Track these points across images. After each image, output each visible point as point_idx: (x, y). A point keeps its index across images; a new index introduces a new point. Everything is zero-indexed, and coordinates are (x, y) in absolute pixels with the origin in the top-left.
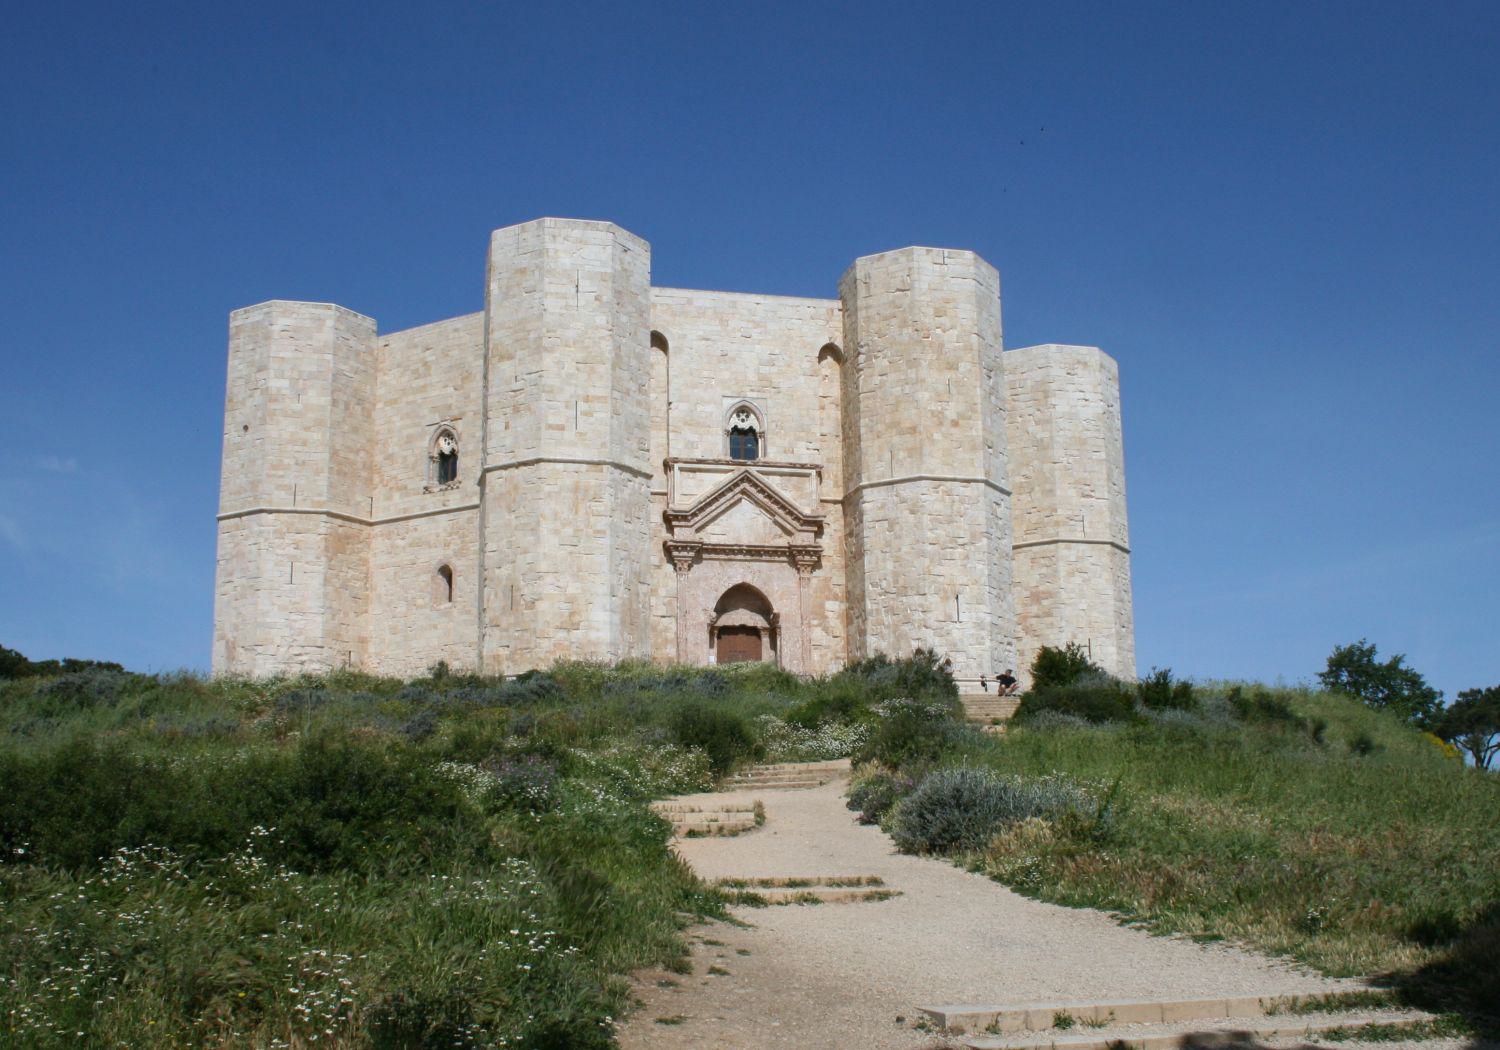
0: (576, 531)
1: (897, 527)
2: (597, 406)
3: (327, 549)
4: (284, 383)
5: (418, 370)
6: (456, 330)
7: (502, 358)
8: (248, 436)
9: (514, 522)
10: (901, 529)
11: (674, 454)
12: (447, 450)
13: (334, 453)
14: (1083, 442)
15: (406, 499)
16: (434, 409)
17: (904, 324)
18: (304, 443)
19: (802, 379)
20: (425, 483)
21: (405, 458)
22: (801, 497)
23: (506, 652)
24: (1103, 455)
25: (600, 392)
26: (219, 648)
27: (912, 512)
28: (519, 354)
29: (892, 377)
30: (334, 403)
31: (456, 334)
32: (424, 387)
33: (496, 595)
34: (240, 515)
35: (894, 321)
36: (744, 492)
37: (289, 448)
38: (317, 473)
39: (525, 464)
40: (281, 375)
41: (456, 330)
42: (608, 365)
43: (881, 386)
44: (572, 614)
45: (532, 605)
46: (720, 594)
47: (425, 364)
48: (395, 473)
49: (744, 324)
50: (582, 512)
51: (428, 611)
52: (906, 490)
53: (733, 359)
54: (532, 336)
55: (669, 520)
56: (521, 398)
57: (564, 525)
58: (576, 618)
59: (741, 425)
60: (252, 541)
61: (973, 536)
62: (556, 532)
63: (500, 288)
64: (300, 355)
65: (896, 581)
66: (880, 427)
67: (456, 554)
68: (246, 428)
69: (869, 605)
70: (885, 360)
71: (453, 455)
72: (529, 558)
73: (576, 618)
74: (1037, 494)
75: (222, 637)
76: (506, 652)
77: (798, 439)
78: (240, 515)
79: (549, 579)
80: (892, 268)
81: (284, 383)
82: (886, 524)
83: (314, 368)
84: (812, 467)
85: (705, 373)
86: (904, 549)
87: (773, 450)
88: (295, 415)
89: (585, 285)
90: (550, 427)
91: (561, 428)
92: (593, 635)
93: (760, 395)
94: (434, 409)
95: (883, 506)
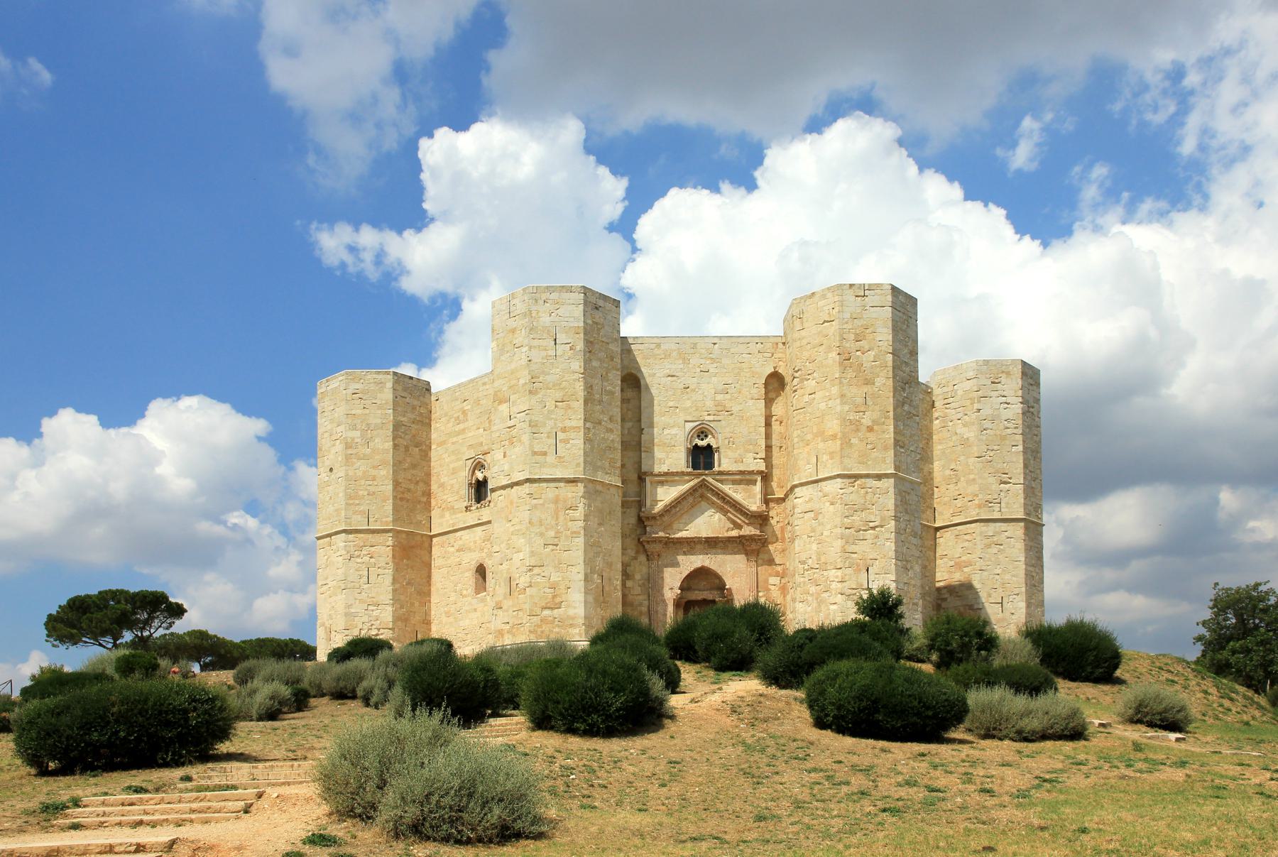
0: (558, 532)
1: (820, 517)
2: (573, 435)
3: (394, 556)
4: (358, 433)
6: (484, 384)
7: (501, 402)
11: (644, 468)
12: (480, 476)
13: (396, 484)
14: (1003, 438)
18: (374, 480)
19: (751, 402)
20: (466, 504)
21: (452, 486)
22: (749, 497)
23: (508, 627)
24: (1020, 448)
25: (574, 423)
26: (320, 632)
27: (832, 504)
30: (395, 446)
34: (330, 535)
36: (702, 496)
37: (363, 482)
38: (384, 501)
41: (484, 384)
42: (582, 401)
43: (810, 403)
44: (554, 597)
46: (684, 575)
47: (464, 412)
49: (703, 361)
50: (561, 518)
53: (693, 390)
54: (522, 381)
55: (643, 522)
56: (514, 432)
57: (547, 530)
58: (558, 600)
59: (701, 443)
61: (883, 519)
62: (542, 534)
64: (367, 411)
65: (819, 559)
66: (809, 437)
68: (331, 470)
71: (485, 481)
72: (521, 555)
73: (558, 600)
74: (962, 484)
75: (323, 625)
77: (748, 451)
78: (330, 535)
79: (536, 570)
81: (358, 433)
82: (812, 514)
83: (379, 421)
84: (760, 473)
85: (671, 404)
86: (826, 533)
87: (724, 462)
88: (365, 457)
89: (562, 338)
90: (535, 453)
91: (545, 454)
92: (571, 612)
93: (716, 418)
95: (811, 500)
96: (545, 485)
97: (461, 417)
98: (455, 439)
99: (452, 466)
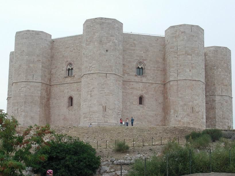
4: (117, 41)
5: (132, 45)
7: (188, 55)
8: (108, 53)
9: (193, 93)
10: (224, 105)
12: (140, 67)
15: (129, 77)
16: (138, 56)
17: (225, 63)
20: (135, 74)
21: (129, 66)
23: (192, 122)
27: (226, 102)
28: (193, 55)
29: (222, 73)
31: (144, 39)
32: (134, 50)
33: (188, 108)
35: (223, 62)
39: (195, 80)
40: (116, 39)
41: (144, 38)
44: (203, 115)
45: (198, 112)
47: (134, 44)
48: (125, 69)
51: (137, 106)
52: (225, 98)
60: (111, 81)
63: (187, 38)
65: (223, 116)
66: (219, 83)
67: (145, 93)
68: (107, 51)
69: (217, 120)
70: (221, 70)
72: (197, 102)
76: (192, 122)
80: (222, 50)
86: (224, 110)
94: (138, 56)
96: (201, 83)
97: (133, 45)
98: (130, 51)
99: (129, 59)
